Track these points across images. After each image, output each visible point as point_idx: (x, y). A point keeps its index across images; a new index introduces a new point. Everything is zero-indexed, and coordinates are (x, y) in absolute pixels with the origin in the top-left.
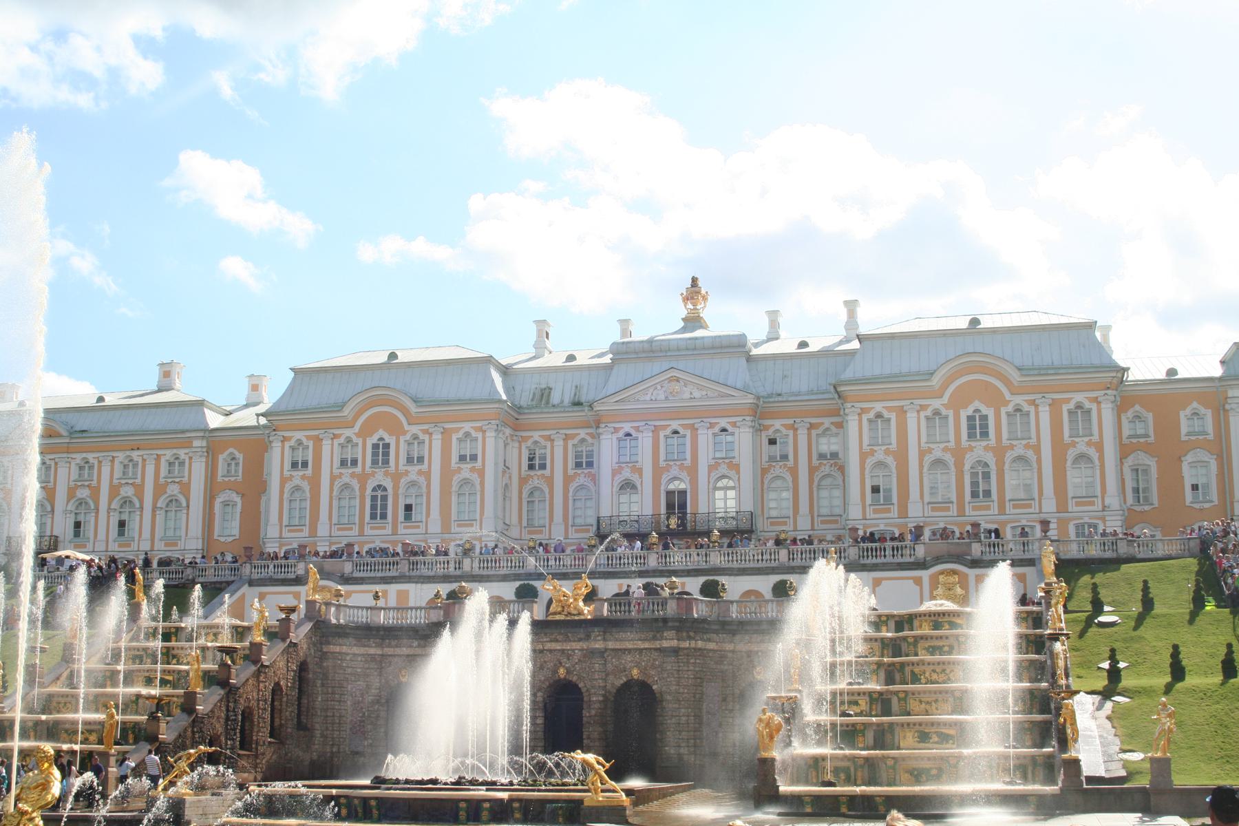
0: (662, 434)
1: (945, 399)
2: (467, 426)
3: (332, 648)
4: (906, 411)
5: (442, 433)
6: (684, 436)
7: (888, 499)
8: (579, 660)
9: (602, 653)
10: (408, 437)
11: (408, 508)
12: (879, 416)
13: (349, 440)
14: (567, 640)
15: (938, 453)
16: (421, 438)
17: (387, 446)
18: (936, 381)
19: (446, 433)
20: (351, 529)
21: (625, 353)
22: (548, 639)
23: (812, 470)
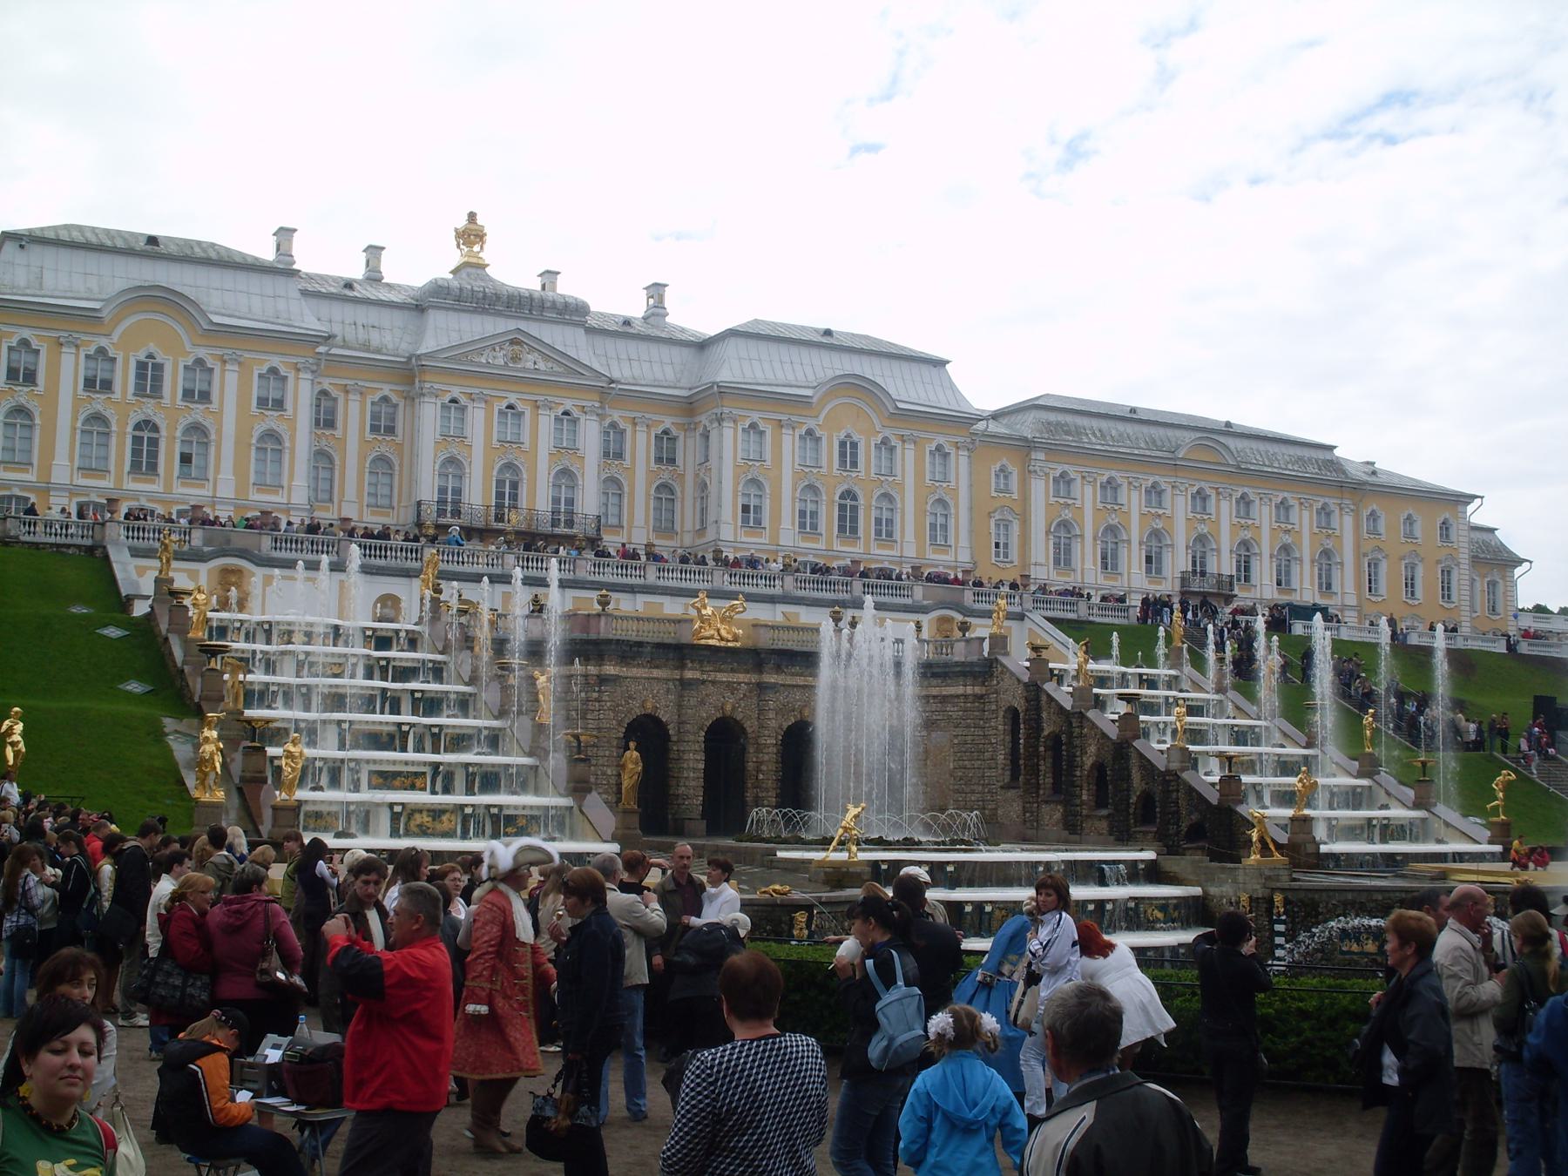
2: (275, 361)
4: (782, 426)
5: (240, 364)
6: (520, 415)
7: (758, 522)
8: (745, 695)
9: (773, 687)
11: (186, 459)
12: (753, 426)
13: (101, 351)
14: (733, 671)
16: (210, 366)
17: (158, 368)
20: (104, 478)
22: (711, 668)
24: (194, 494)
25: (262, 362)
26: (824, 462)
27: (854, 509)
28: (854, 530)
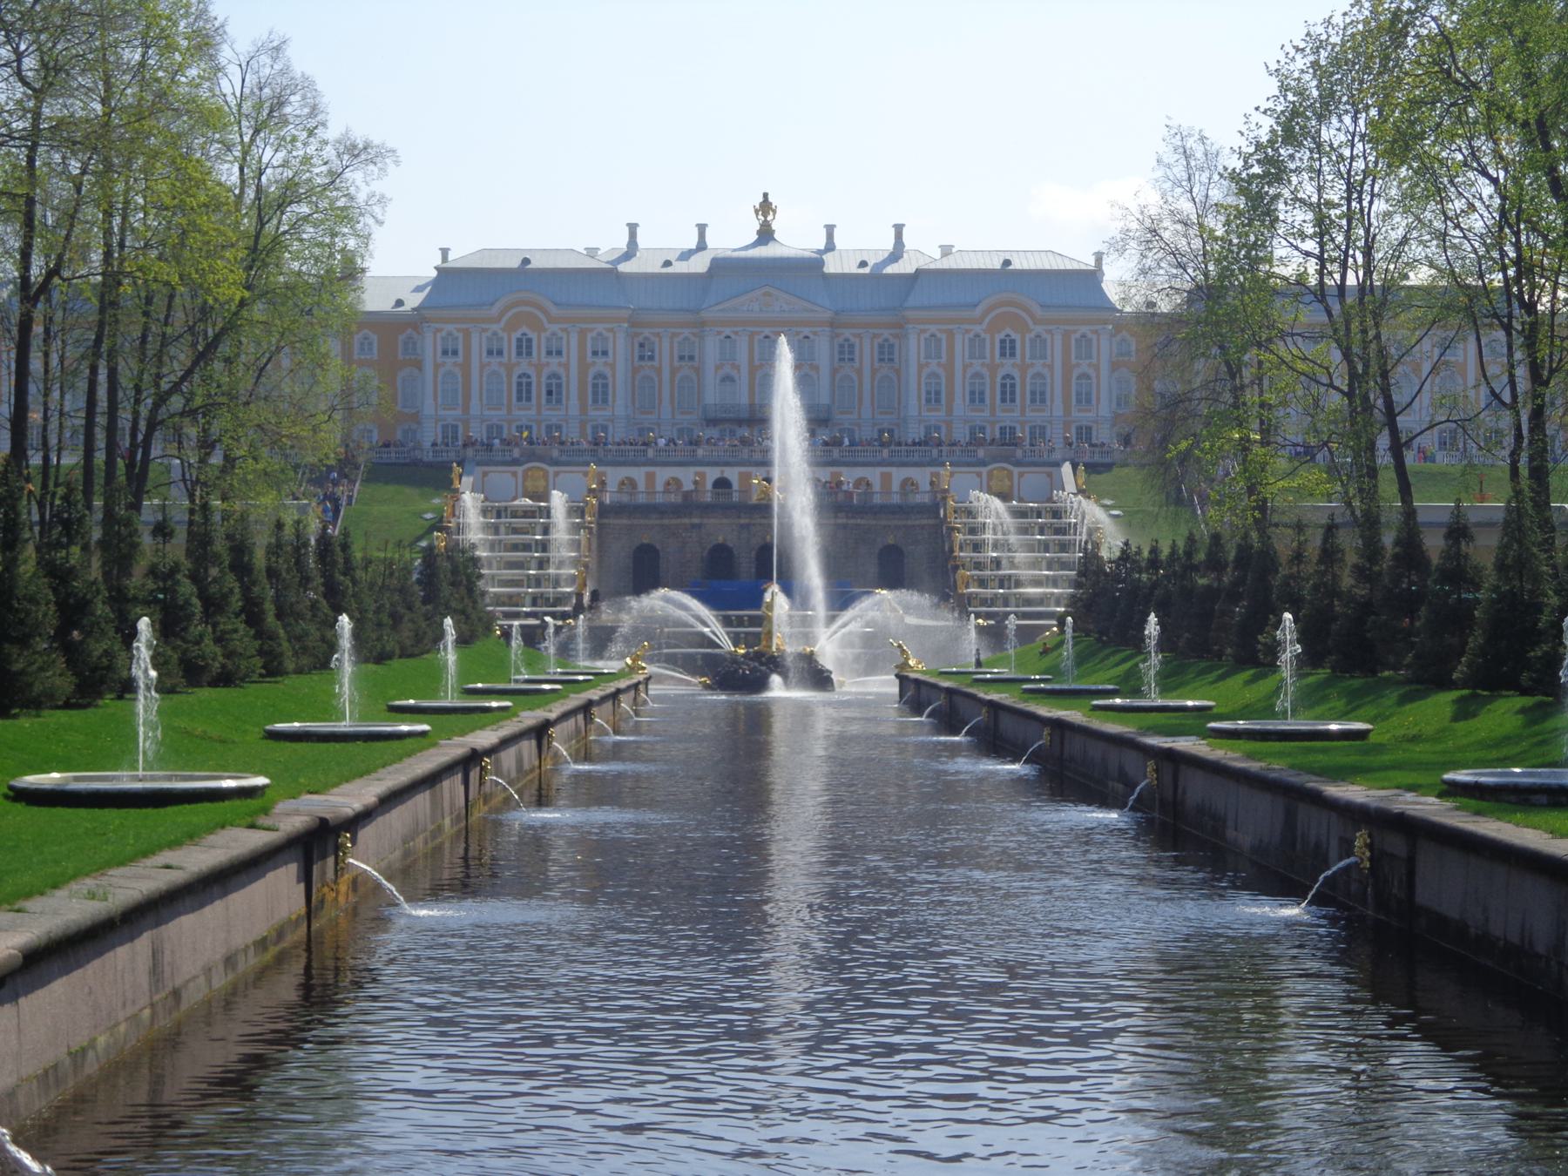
0: (757, 338)
1: (984, 326)
3: (606, 521)
10: (548, 334)
13: (495, 334)
15: (977, 365)
18: (978, 311)
19: (582, 333)
21: (722, 266)
23: (874, 371)
24: (552, 415)
25: (592, 330)
26: (988, 355)
27: (1013, 386)
28: (1013, 400)
